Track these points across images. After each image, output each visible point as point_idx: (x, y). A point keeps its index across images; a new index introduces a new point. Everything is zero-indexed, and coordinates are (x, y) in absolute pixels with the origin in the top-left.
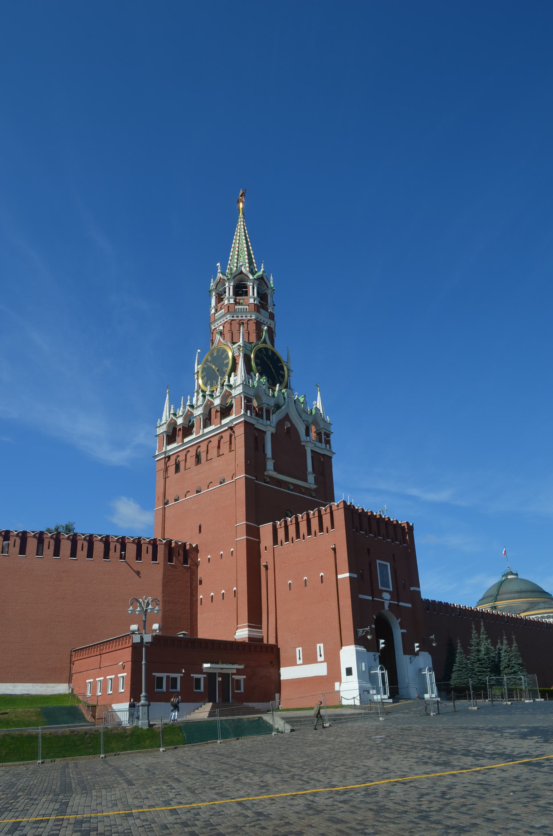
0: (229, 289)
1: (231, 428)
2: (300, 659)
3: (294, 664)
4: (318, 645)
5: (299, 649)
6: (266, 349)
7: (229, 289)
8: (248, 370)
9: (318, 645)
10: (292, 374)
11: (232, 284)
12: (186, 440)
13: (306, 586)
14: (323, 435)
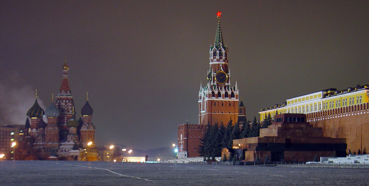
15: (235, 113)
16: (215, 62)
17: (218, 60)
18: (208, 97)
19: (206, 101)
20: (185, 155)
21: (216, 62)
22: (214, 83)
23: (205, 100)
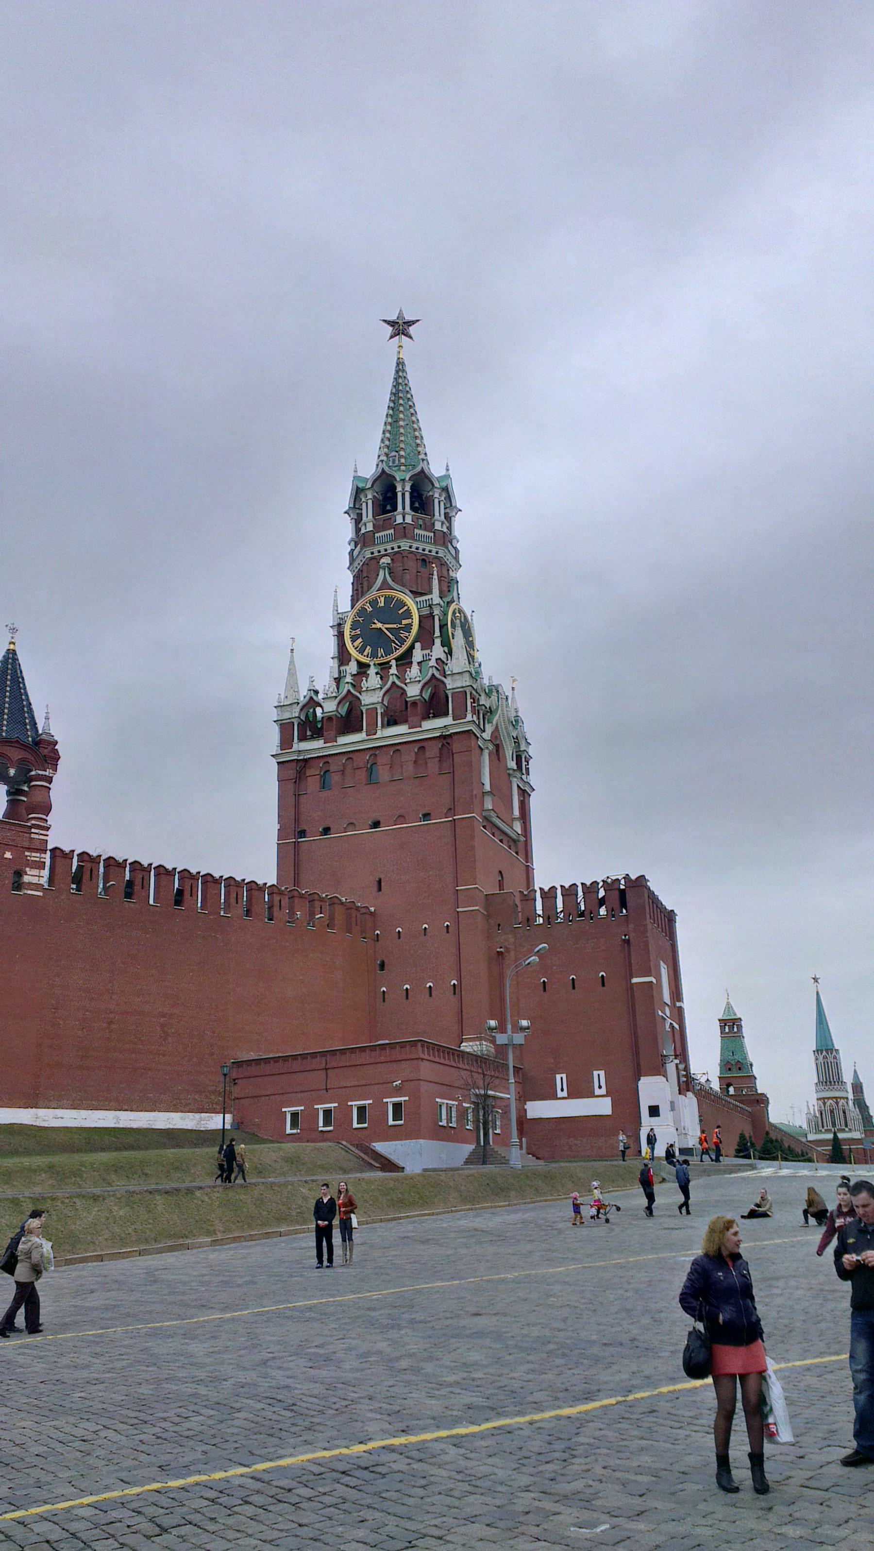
0: (403, 495)
1: (443, 737)
2: (562, 1090)
3: (554, 1097)
4: (596, 1073)
5: (561, 1079)
7: (403, 495)
9: (596, 1073)
11: (408, 488)
12: (342, 740)
13: (574, 988)
14: (523, 760)
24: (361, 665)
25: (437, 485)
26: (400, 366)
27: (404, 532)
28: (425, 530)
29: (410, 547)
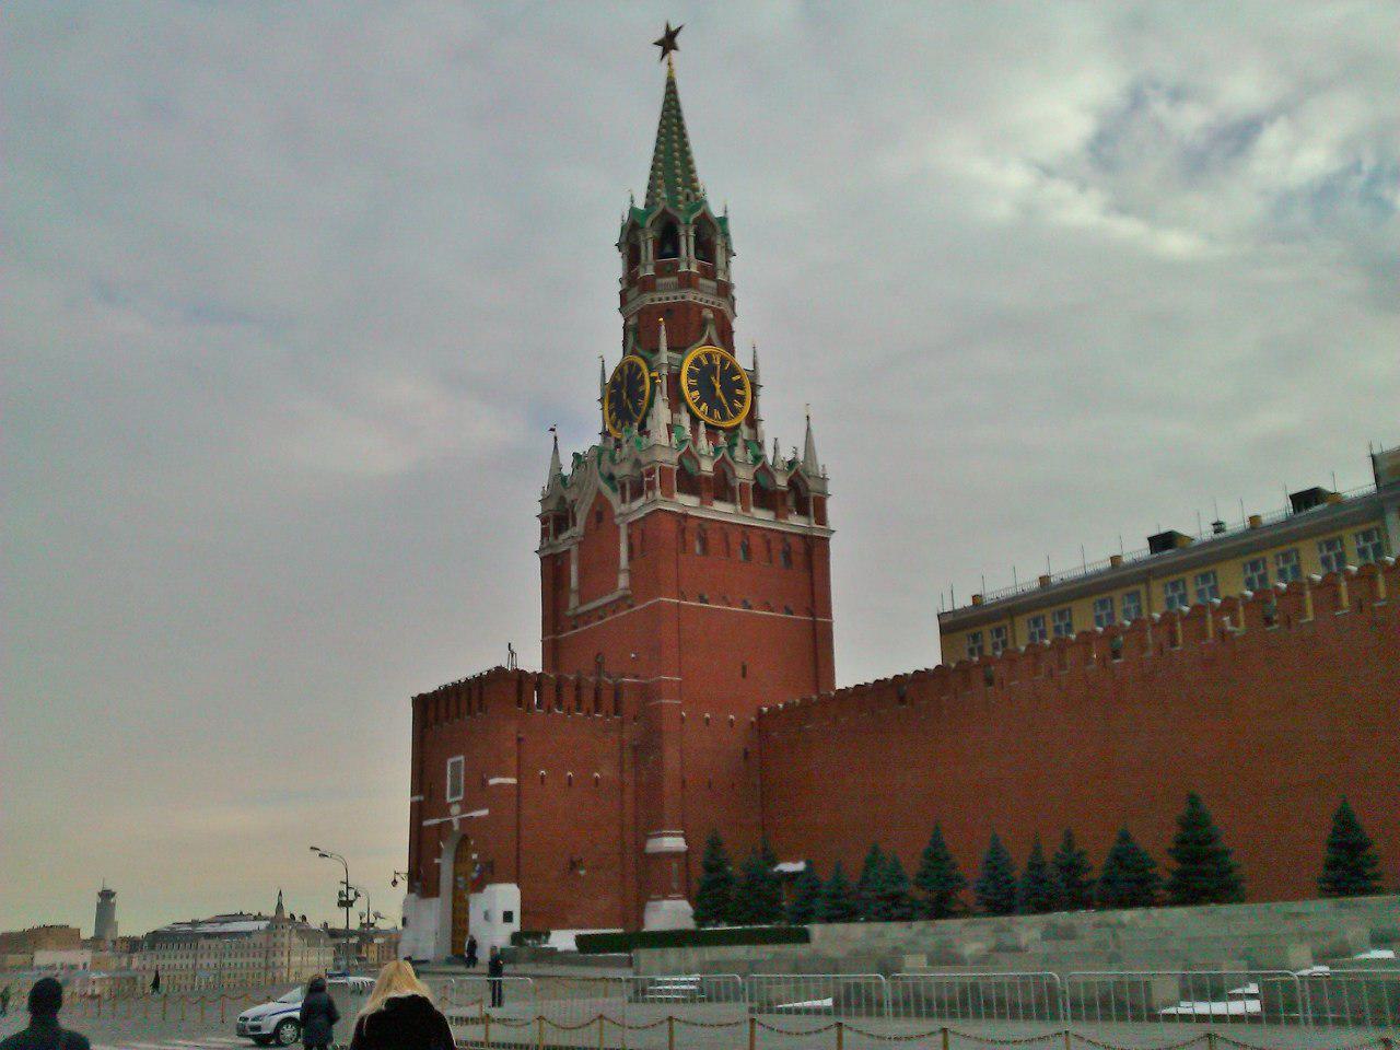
0: (646, 243)
6: (709, 356)
8: (676, 400)
10: (761, 392)
15: (812, 615)
16: (671, 294)
17: (687, 281)
18: (658, 493)
19: (631, 525)
20: (508, 917)
21: (677, 294)
22: (675, 416)
23: (617, 521)
24: (617, 440)
25: (682, 221)
26: (671, 87)
27: (647, 285)
28: (671, 276)
29: (653, 300)
